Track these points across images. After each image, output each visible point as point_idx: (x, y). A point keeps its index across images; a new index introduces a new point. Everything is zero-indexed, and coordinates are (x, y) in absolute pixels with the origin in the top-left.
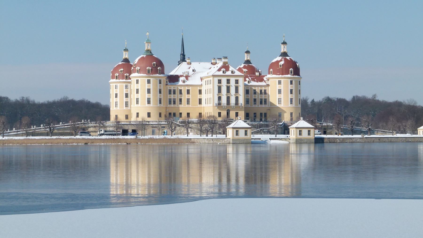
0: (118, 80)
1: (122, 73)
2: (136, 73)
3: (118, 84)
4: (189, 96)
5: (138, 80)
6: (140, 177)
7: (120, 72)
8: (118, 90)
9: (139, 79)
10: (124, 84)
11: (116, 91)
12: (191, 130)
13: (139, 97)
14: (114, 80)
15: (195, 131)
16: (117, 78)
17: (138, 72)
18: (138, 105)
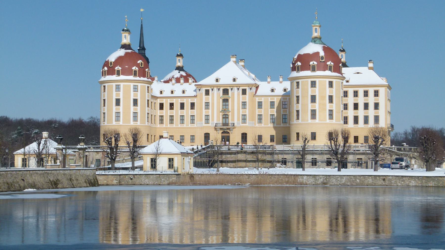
0: (138, 78)
1: (112, 66)
2: (327, 71)
3: (139, 85)
4: (378, 111)
5: (315, 82)
6: (247, 233)
7: (141, 66)
8: (139, 93)
9: (334, 81)
10: (132, 84)
11: (119, 95)
12: (415, 162)
13: (334, 109)
14: (114, 77)
15: (419, 162)
16: (135, 75)
17: (330, 70)
18: (333, 121)
